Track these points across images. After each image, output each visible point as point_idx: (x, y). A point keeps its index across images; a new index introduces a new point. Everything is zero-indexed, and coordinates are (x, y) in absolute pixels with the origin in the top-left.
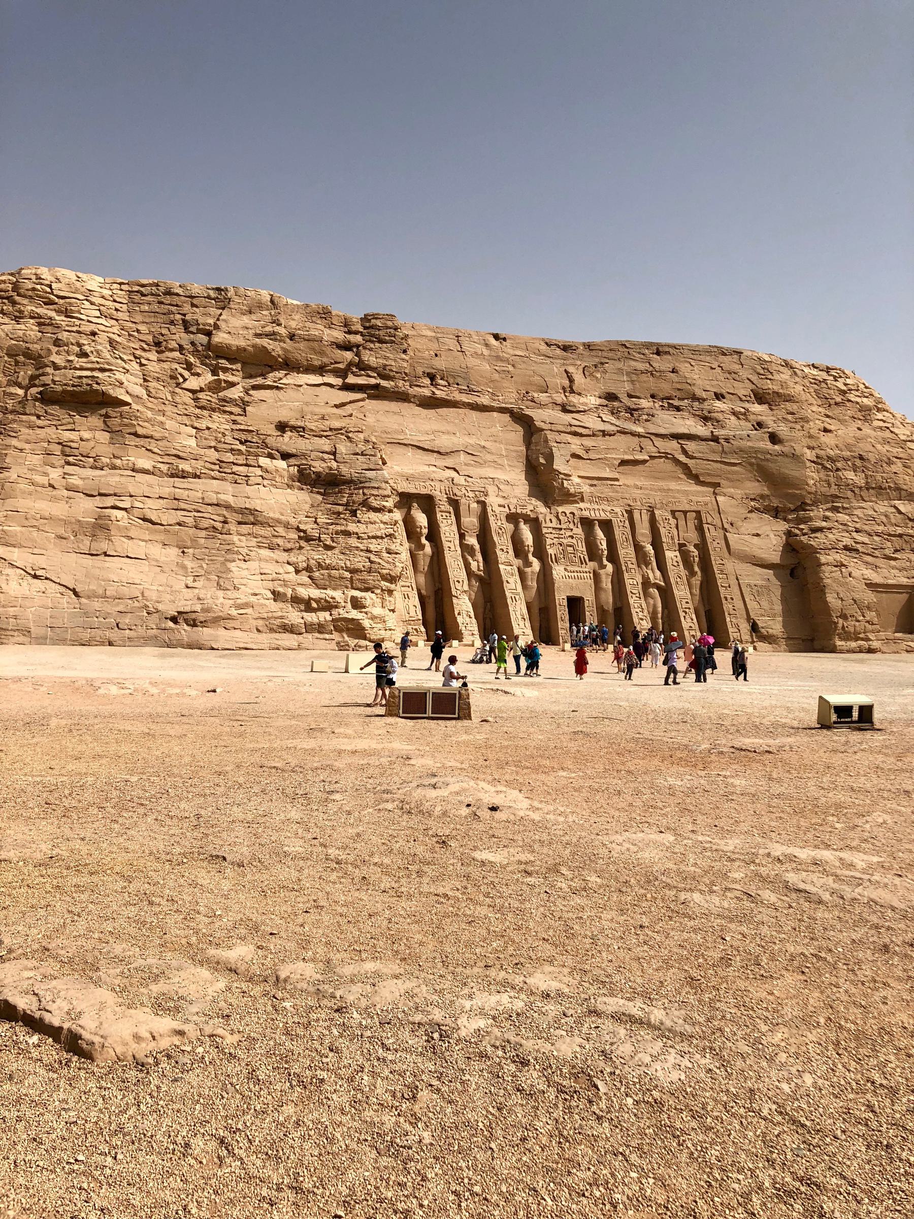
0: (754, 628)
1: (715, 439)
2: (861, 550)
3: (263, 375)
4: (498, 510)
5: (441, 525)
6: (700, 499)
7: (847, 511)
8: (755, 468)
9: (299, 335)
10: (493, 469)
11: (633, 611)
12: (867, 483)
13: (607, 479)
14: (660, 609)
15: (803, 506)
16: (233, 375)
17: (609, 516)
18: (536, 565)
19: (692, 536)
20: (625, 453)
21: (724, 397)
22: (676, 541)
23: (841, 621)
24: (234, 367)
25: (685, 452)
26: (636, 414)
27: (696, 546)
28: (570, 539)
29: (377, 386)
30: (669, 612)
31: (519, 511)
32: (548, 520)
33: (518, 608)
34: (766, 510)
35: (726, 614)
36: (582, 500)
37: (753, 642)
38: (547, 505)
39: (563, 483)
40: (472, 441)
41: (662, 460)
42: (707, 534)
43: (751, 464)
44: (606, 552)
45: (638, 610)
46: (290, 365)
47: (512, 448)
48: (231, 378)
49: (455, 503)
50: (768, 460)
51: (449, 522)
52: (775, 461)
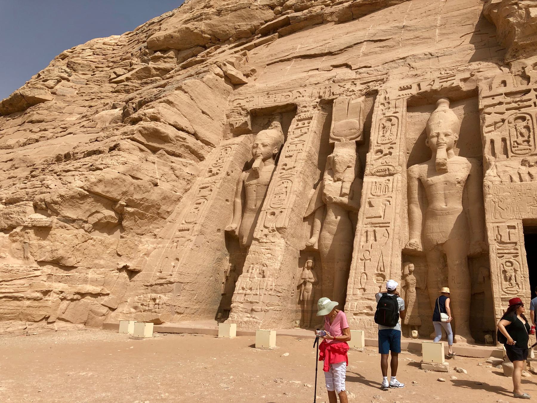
3: (196, 56)
4: (393, 94)
5: (290, 136)
9: (226, 10)
10: (409, 48)
16: (165, 62)
18: (459, 167)
24: (165, 56)
29: (287, 22)
31: (437, 86)
33: (375, 255)
38: (503, 62)
39: (528, 13)
40: (383, 27)
46: (218, 40)
47: (456, 13)
48: (162, 65)
49: (327, 105)
51: (304, 130)
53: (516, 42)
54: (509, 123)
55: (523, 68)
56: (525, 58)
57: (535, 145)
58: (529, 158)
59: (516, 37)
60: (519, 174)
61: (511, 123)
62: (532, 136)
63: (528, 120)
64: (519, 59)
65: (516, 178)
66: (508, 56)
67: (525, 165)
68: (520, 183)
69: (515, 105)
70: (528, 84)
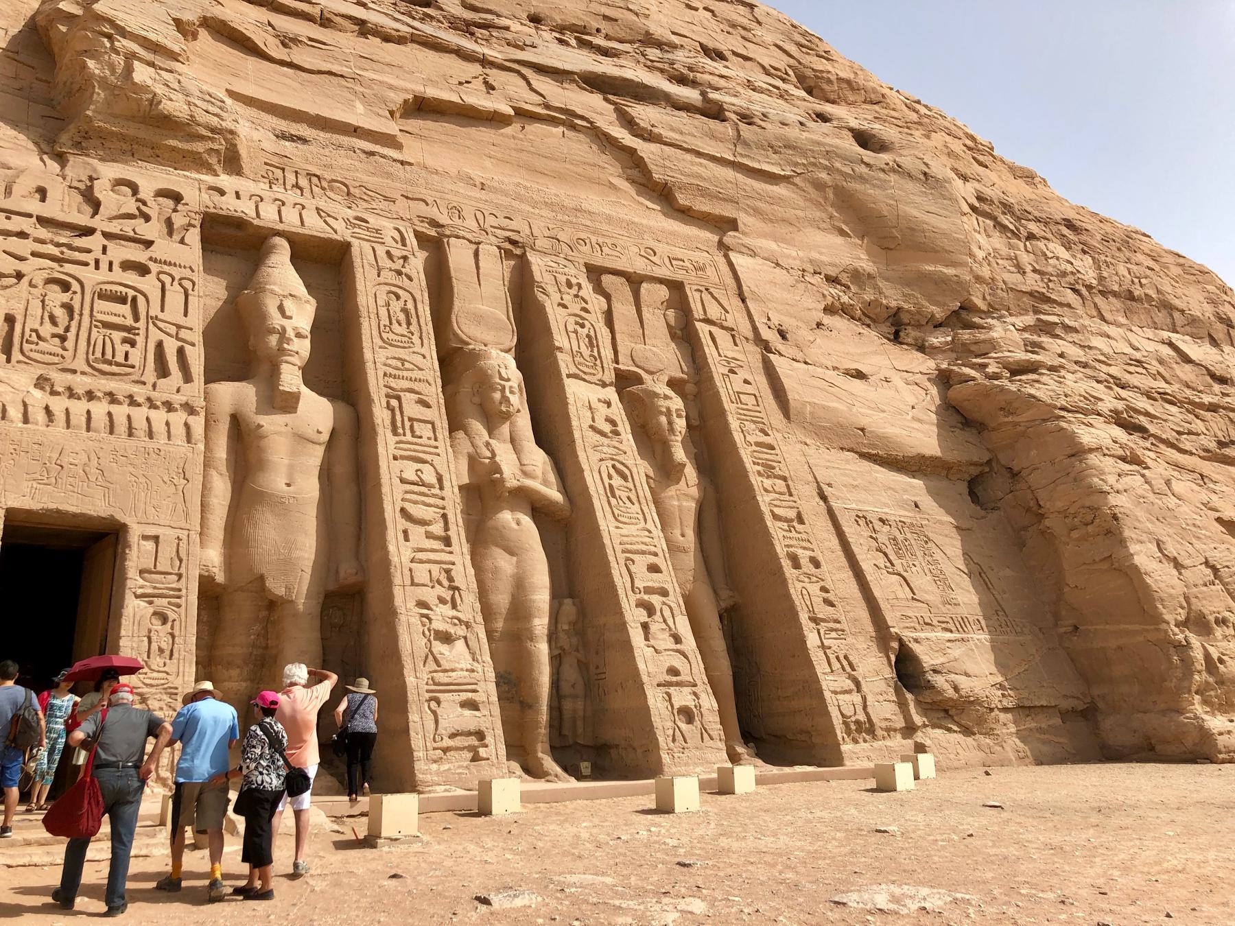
0: (907, 672)
1: (715, 112)
2: (1152, 429)
6: (679, 252)
7: (1075, 337)
8: (830, 194)
11: (404, 600)
12: (1101, 279)
13: (356, 131)
14: (541, 596)
15: (962, 316)
17: (342, 232)
19: (660, 357)
20: (430, 81)
21: (720, 56)
22: (609, 365)
23: (1195, 641)
25: (629, 123)
26: (479, 32)
27: (672, 383)
28: (131, 278)
30: (582, 612)
32: (24, 185)
34: (870, 316)
35: (804, 617)
36: (232, 163)
37: (909, 730)
39: (129, 70)
41: (561, 129)
42: (709, 350)
43: (819, 186)
44: (302, 348)
45: (430, 595)
50: (862, 179)
52: (883, 186)
53: (88, 116)
54: (31, 285)
55: (91, 179)
56: (100, 160)
57: (75, 351)
58: (55, 375)
59: (92, 107)
60: (25, 405)
61: (35, 287)
62: (73, 330)
63: (75, 293)
64: (87, 155)
65: (15, 413)
66: (64, 138)
67: (42, 389)
68: (20, 425)
69: (55, 251)
70: (92, 217)
